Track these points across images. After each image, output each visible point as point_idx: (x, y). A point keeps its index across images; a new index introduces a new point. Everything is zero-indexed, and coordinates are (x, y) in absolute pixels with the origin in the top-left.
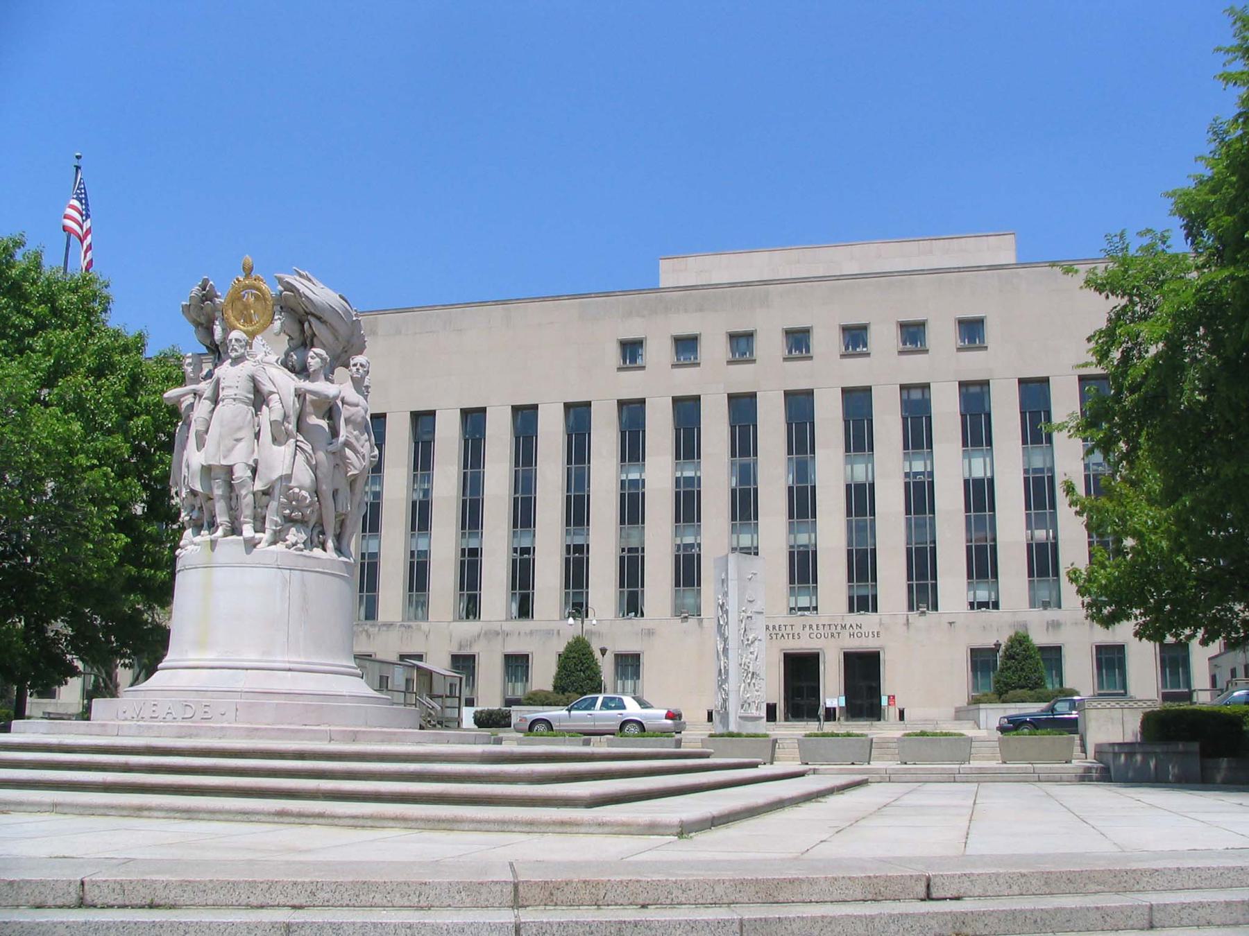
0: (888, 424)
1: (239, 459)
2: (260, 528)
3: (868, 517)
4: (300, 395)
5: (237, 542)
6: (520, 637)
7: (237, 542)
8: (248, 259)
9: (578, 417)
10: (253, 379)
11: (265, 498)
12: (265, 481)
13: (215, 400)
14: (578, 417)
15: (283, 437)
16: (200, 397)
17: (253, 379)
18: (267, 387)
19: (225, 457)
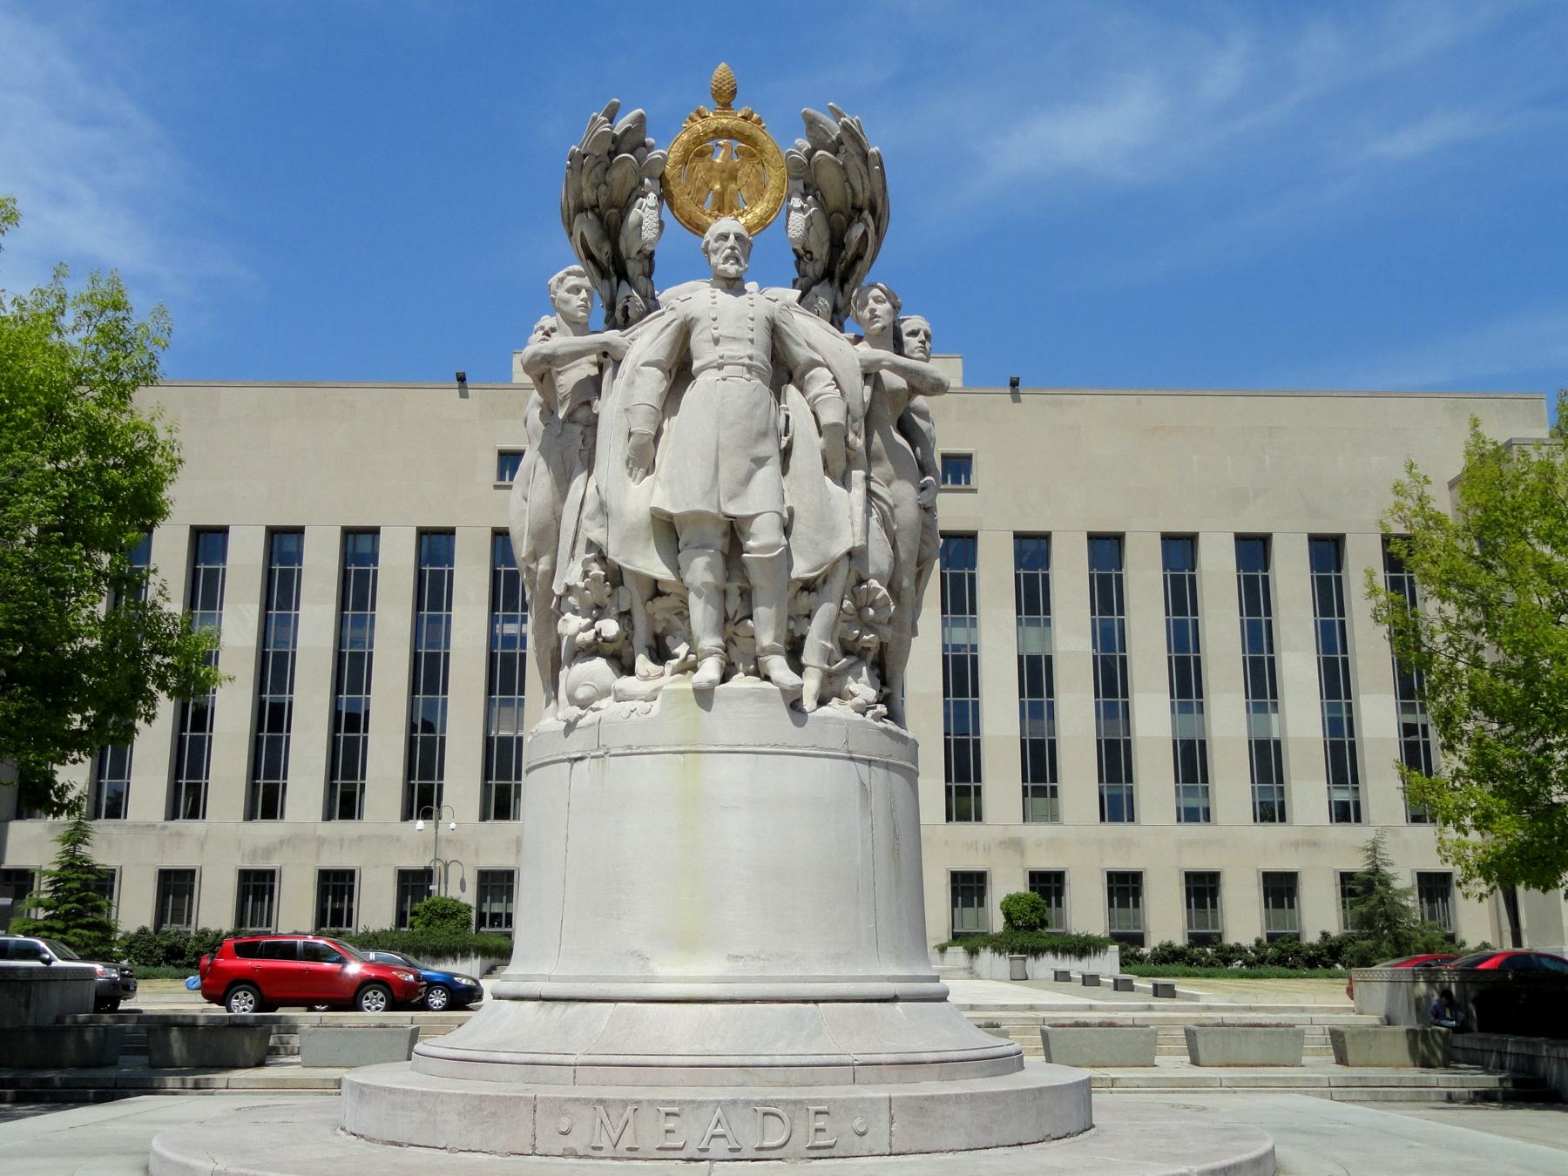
0: (995, 574)
1: (758, 501)
2: (798, 668)
3: (970, 699)
4: (870, 375)
5: (763, 697)
6: (341, 845)
7: (763, 697)
9: (435, 545)
10: (775, 331)
11: (805, 599)
12: (816, 559)
13: (680, 371)
14: (435, 545)
15: (840, 465)
16: (618, 363)
17: (775, 331)
18: (802, 353)
19: (732, 497)
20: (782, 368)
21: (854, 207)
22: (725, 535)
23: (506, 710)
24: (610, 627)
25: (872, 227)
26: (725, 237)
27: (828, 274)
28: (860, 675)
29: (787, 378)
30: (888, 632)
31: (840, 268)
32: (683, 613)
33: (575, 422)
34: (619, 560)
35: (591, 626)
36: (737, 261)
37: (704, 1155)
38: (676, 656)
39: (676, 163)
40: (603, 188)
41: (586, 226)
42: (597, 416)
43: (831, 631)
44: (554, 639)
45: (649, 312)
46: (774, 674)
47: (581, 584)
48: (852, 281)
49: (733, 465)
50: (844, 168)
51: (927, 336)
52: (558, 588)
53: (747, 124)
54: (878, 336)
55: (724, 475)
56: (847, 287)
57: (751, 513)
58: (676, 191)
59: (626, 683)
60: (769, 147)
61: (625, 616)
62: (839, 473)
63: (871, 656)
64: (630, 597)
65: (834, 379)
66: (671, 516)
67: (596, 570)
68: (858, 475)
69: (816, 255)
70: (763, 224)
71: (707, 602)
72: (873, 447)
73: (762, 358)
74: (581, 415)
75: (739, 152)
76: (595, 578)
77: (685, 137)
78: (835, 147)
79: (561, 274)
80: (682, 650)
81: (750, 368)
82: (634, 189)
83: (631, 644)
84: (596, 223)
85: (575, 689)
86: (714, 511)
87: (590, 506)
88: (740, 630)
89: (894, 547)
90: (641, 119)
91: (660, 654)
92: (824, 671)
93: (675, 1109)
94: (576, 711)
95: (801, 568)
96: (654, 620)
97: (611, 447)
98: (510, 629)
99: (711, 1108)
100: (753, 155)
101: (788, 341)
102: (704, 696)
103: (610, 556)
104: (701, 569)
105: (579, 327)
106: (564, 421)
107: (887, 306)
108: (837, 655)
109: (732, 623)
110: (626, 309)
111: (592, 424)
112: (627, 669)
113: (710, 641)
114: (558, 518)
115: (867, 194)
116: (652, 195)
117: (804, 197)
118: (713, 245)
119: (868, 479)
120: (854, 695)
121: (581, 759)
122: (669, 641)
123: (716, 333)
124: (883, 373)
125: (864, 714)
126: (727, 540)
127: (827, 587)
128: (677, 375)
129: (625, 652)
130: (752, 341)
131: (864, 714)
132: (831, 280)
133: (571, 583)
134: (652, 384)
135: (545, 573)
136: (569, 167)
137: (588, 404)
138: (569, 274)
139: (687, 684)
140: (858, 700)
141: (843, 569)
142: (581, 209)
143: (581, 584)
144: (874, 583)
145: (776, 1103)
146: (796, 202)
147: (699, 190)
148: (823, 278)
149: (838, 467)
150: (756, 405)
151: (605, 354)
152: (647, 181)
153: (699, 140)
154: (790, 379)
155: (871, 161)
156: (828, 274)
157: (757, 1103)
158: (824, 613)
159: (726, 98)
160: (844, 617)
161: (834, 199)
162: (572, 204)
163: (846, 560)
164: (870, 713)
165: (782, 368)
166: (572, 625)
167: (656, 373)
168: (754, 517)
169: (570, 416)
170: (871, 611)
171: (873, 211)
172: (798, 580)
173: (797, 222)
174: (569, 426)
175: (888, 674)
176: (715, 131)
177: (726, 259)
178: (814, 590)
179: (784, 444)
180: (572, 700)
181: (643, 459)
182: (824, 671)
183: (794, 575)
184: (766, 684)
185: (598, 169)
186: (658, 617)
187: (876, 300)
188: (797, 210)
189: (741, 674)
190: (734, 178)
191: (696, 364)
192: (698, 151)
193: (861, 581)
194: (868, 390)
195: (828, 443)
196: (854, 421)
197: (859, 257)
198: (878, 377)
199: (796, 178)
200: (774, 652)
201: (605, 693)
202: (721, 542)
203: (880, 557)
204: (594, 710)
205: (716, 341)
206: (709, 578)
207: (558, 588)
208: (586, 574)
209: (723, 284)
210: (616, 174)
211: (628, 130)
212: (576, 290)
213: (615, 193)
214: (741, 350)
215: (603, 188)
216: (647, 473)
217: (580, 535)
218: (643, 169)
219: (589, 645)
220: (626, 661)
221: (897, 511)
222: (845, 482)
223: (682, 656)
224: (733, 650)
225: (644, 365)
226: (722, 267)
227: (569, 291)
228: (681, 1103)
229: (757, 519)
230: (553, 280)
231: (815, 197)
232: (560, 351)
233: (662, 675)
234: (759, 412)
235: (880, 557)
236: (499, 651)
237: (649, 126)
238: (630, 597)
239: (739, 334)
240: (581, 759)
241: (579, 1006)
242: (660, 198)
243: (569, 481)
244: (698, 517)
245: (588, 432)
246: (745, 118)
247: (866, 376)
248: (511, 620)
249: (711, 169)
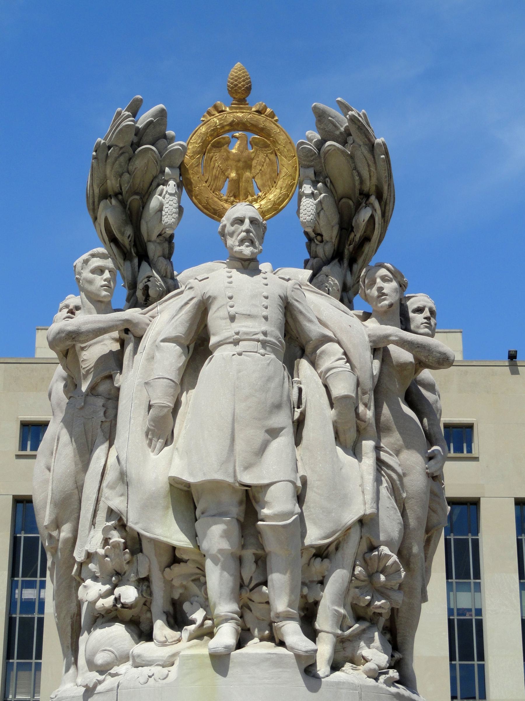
1: (272, 470)
4: (379, 350)
8: (237, 68)
10: (288, 308)
11: (318, 565)
12: (329, 527)
15: (352, 435)
16: (139, 339)
17: (288, 308)
18: (314, 330)
19: (247, 467)
20: (295, 344)
21: (361, 193)
22: (240, 503)
23: (23, 674)
24: (129, 593)
25: (379, 212)
26: (240, 221)
27: (337, 255)
28: (372, 640)
29: (299, 353)
30: (399, 598)
31: (348, 250)
32: (200, 579)
33: (98, 395)
34: (138, 528)
35: (111, 592)
36: (252, 243)
38: (193, 622)
39: (195, 153)
40: (126, 176)
41: (109, 211)
42: (118, 389)
43: (344, 597)
44: (74, 605)
45: (169, 291)
46: (289, 640)
47: (102, 552)
48: (360, 261)
49: (249, 436)
50: (352, 157)
51: (432, 312)
52: (79, 555)
53: (261, 118)
54: (385, 312)
55: (240, 446)
56: (355, 267)
57: (266, 481)
58: (194, 179)
59: (144, 648)
60: (282, 138)
61: (144, 583)
62: (350, 443)
63: (382, 621)
64: (149, 563)
65: (345, 354)
66: (188, 485)
67: (116, 537)
68: (368, 445)
69: (326, 237)
70: (276, 208)
71: (224, 568)
72: (383, 418)
73: (275, 334)
74: (103, 388)
75: (253, 143)
76: (115, 546)
77: (203, 129)
78: (344, 138)
79: (85, 256)
80: (198, 615)
81: (264, 344)
82: (155, 177)
83: (149, 610)
84: (119, 209)
85: (94, 654)
86: (230, 480)
87: (111, 476)
88: (255, 596)
89: (404, 514)
90: (162, 114)
91: (177, 620)
92: (337, 636)
94: (95, 676)
95: (314, 536)
96: (172, 587)
97: (132, 419)
98: (29, 594)
100: (266, 146)
101: (301, 318)
102: (220, 662)
103: (130, 524)
104: (217, 537)
105: (102, 306)
106: (87, 395)
107: (394, 284)
108: (349, 620)
109: (248, 589)
110: (146, 288)
111: (114, 396)
112: (146, 635)
113: (226, 607)
114: (79, 488)
115: (374, 181)
116: (172, 183)
117: (314, 184)
118: (229, 228)
119: (378, 448)
120: (366, 660)
122: (186, 606)
123: (232, 311)
124: (392, 347)
125: (376, 679)
126: (243, 507)
127: (339, 554)
128: (196, 349)
129: (144, 617)
130: (266, 318)
131: (376, 679)
132: (341, 261)
133: (92, 551)
134: (172, 358)
135: (66, 541)
136: (95, 158)
137: (110, 377)
138: (93, 256)
139: (203, 649)
140: (371, 665)
141: (355, 536)
142: (105, 196)
143: (102, 552)
144: (385, 550)
146: (307, 189)
147: (216, 178)
148: (333, 258)
149: (350, 437)
150: (269, 379)
152: (167, 170)
153: (216, 132)
154: (303, 354)
155: (377, 151)
156: (337, 255)
158: (337, 579)
159: (241, 94)
160: (355, 583)
161: (343, 184)
162: (97, 191)
163: (358, 527)
164: (382, 678)
165: (295, 344)
166: (92, 591)
167: (175, 349)
168: (268, 486)
169: (92, 389)
170: (382, 578)
171: (380, 197)
172: (312, 546)
173: (308, 207)
174: (92, 399)
175: (399, 639)
176: (231, 124)
177: (242, 242)
178: (327, 557)
179: (297, 415)
180: (91, 665)
181: (161, 430)
182: (337, 636)
183: (308, 541)
184: (281, 650)
185: (122, 159)
186: (176, 583)
187: (384, 279)
188: (308, 196)
189: (256, 640)
190: (248, 166)
191: (213, 340)
192: (215, 141)
193: (373, 548)
194: (377, 364)
195: (339, 414)
196: (364, 393)
197: (366, 239)
198: (386, 351)
199: (308, 167)
200: (288, 617)
201: (123, 658)
202: (236, 510)
203: (390, 525)
204: (113, 675)
205: (232, 318)
206: (225, 545)
207: (79, 555)
208: (106, 541)
209: (238, 264)
210: (139, 164)
211: (150, 123)
212: (100, 271)
213: (138, 181)
214: (256, 327)
215: (126, 176)
216: (166, 444)
217: (101, 504)
218: (164, 159)
219: (108, 611)
220: (144, 627)
221: (406, 480)
222: (355, 451)
223: (199, 622)
224: (248, 616)
225: (164, 341)
226: (237, 249)
227: (93, 272)
229: (272, 488)
230: (79, 262)
231: (325, 184)
232: (84, 328)
233: (179, 640)
234: (273, 385)
235: (390, 525)
236: (17, 616)
237: (170, 119)
238: (149, 563)
239: (254, 311)
242: (179, 186)
243: (91, 452)
244: (214, 487)
245: (110, 404)
246: (259, 112)
247: (375, 351)
248: (30, 585)
249: (227, 159)
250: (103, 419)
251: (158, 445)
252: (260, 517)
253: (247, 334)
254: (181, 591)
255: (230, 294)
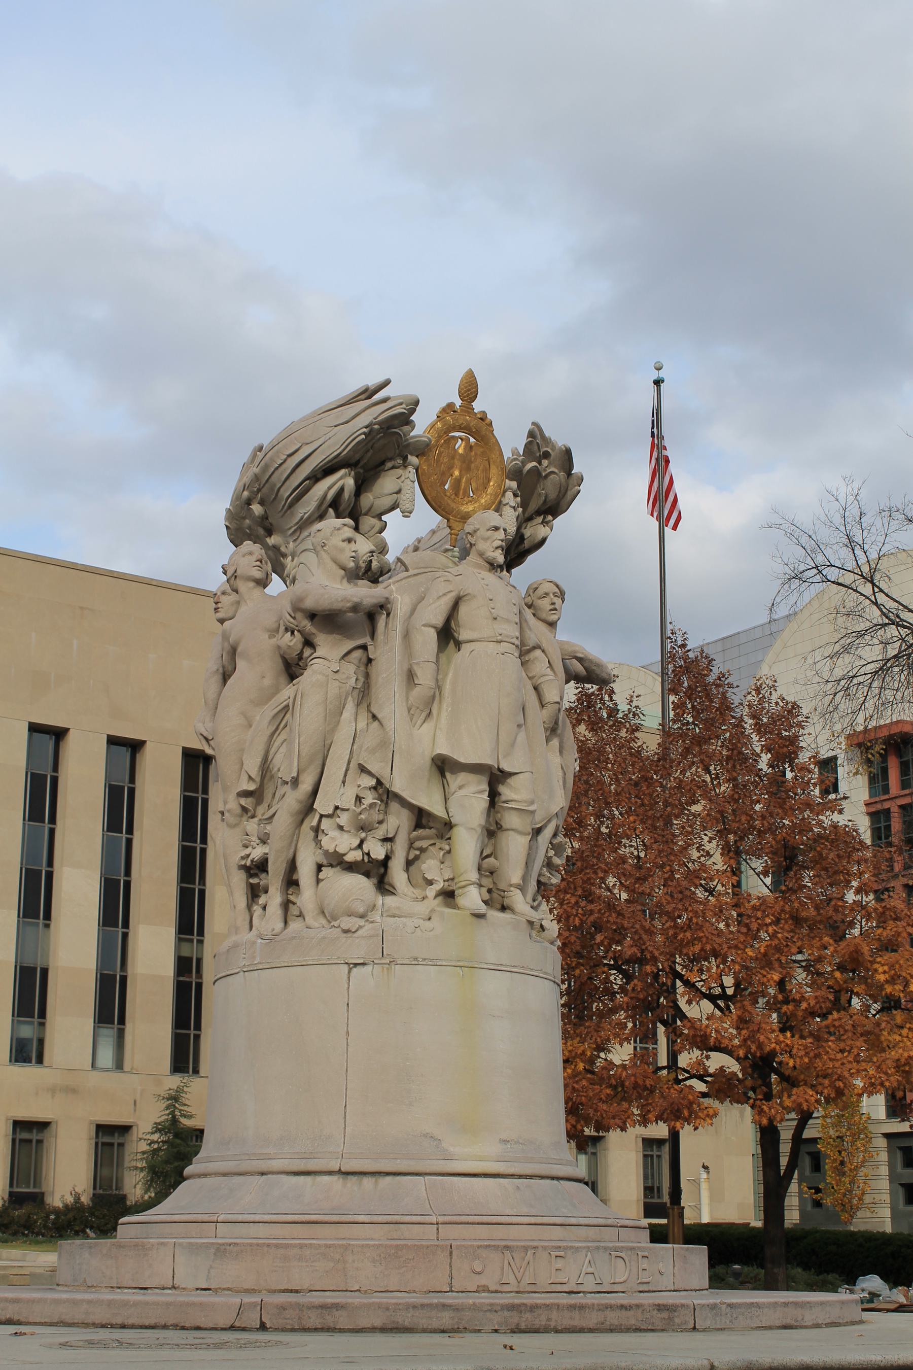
24: (378, 852)
35: (360, 846)
37: (581, 1288)
44: (292, 851)
67: (370, 798)
93: (562, 1253)
99: (584, 1252)
121: (363, 964)
138: (345, 525)
145: (621, 1249)
151: (382, 607)
157: (611, 1249)
208: (359, 799)
225: (424, 625)
228: (565, 1249)
240: (363, 964)
241: (389, 1179)
250: (354, 685)
251: (419, 722)
252: (503, 798)
253: (507, 636)
254: (418, 853)
255: (491, 597)
